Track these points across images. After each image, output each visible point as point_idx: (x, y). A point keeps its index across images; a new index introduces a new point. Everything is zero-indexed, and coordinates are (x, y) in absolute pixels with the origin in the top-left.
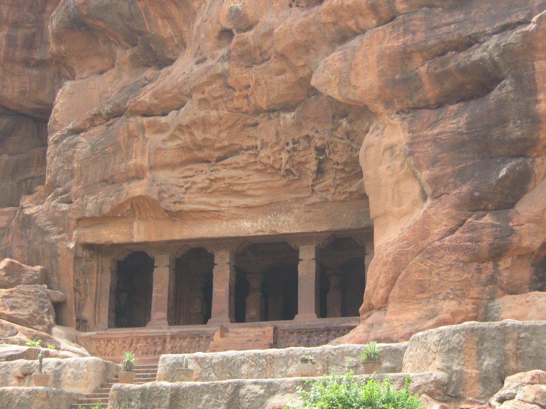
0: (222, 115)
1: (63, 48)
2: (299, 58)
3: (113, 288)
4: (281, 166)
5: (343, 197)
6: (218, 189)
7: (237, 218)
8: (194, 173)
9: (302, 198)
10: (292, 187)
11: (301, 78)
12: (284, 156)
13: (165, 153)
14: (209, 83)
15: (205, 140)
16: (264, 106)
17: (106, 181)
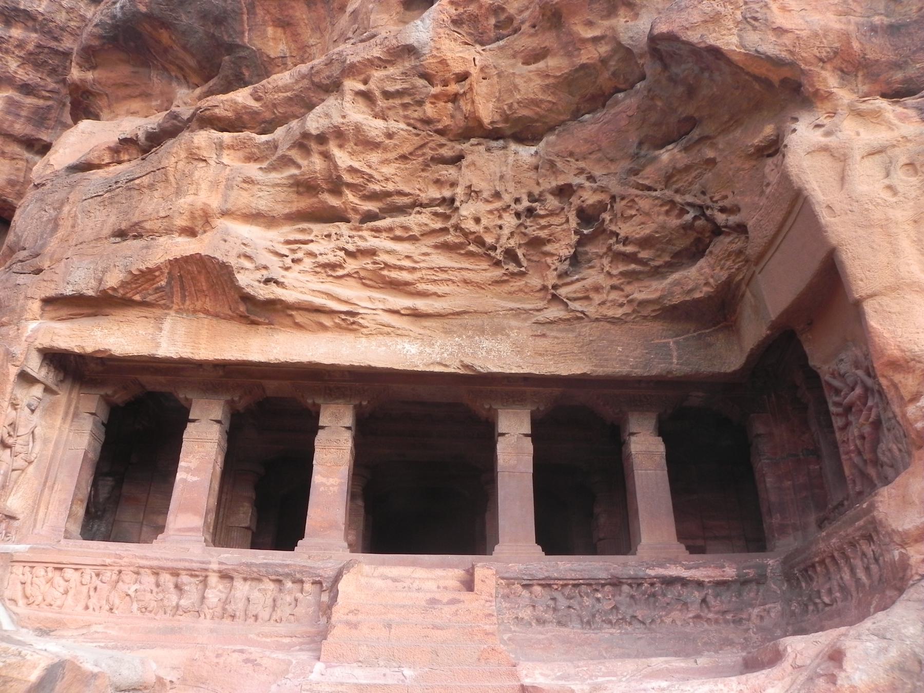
0: (394, 130)
1: (90, 76)
2: (590, 24)
3: (90, 455)
4: (498, 240)
5: (619, 312)
6: (357, 272)
7: (388, 334)
8: (310, 238)
9: (526, 311)
10: (506, 288)
11: (583, 67)
12: (509, 221)
13: (261, 190)
14: (382, 63)
15: (352, 170)
16: (486, 121)
17: (121, 234)
